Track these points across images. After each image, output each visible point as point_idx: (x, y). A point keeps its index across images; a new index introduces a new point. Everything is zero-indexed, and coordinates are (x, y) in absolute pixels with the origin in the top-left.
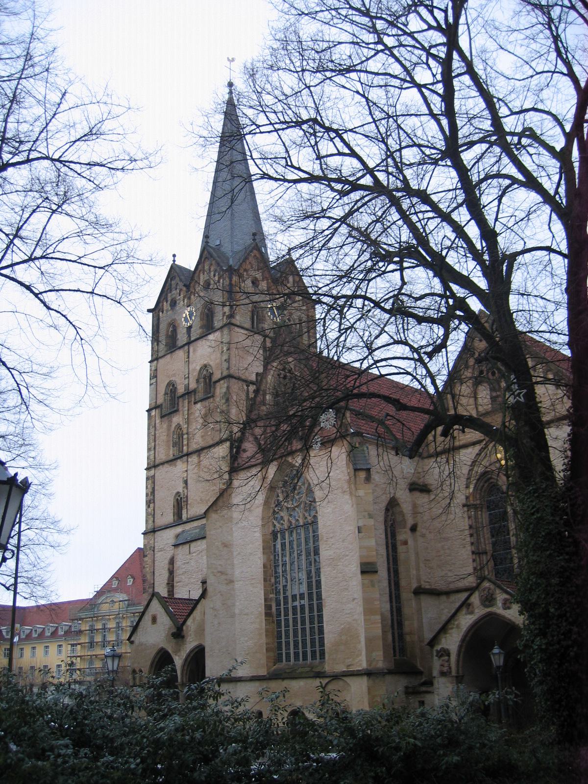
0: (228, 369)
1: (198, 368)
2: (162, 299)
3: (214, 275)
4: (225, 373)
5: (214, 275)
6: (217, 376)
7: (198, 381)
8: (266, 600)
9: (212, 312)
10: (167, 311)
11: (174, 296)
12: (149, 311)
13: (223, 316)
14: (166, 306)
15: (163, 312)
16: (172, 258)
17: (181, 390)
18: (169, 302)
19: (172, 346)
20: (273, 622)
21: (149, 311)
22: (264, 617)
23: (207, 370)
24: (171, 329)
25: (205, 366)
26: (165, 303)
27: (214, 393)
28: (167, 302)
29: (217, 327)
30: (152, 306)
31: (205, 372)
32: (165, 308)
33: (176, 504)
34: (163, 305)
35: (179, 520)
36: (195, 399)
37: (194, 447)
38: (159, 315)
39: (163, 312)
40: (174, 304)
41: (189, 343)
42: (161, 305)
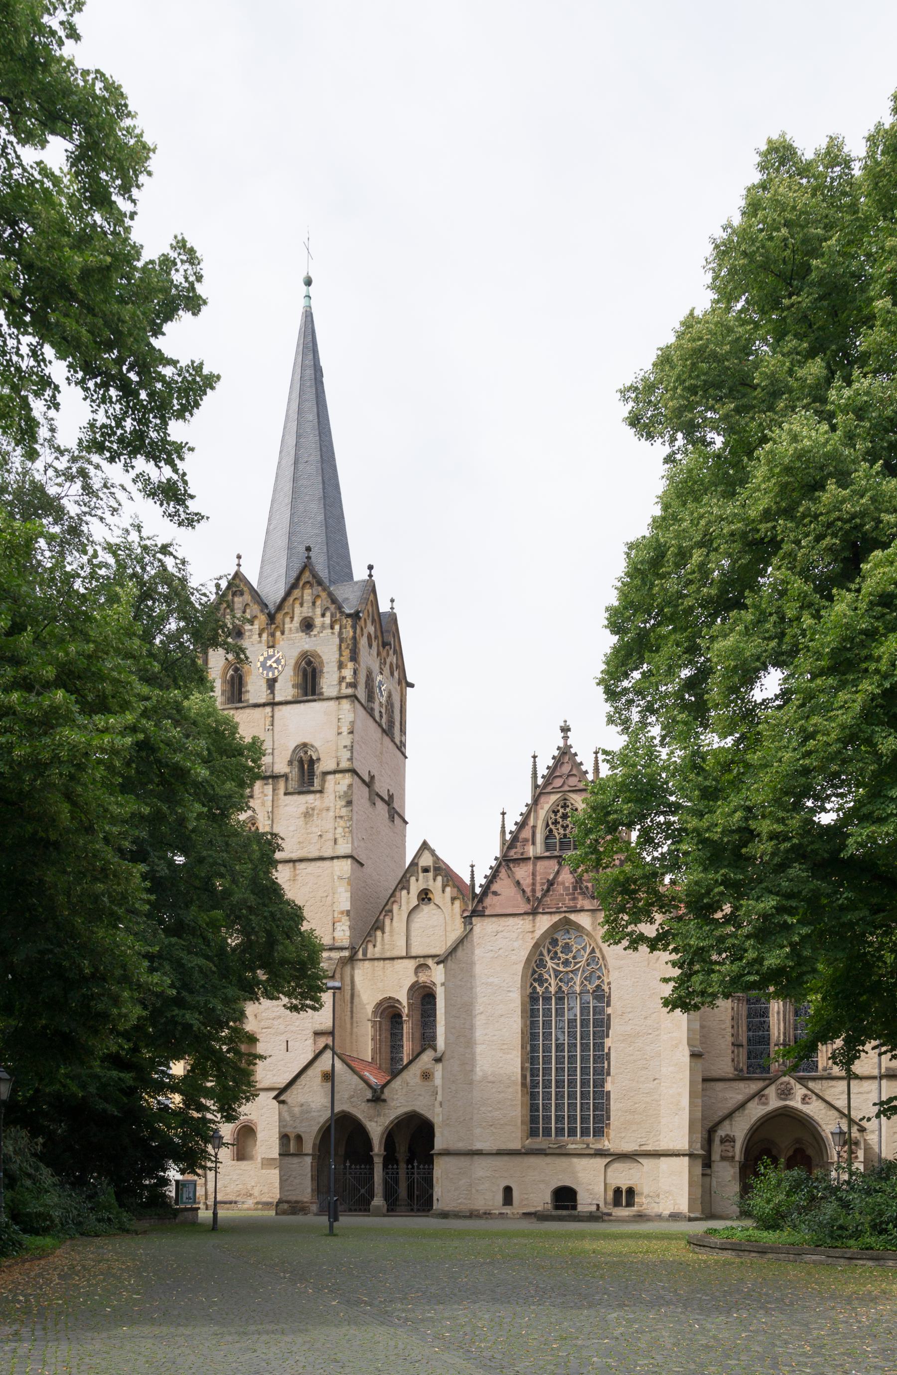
0: (351, 759)
3: (323, 615)
4: (345, 765)
5: (323, 615)
7: (290, 763)
9: (314, 670)
16: (236, 561)
23: (306, 753)
24: (231, 672)
25: (305, 745)
36: (286, 788)
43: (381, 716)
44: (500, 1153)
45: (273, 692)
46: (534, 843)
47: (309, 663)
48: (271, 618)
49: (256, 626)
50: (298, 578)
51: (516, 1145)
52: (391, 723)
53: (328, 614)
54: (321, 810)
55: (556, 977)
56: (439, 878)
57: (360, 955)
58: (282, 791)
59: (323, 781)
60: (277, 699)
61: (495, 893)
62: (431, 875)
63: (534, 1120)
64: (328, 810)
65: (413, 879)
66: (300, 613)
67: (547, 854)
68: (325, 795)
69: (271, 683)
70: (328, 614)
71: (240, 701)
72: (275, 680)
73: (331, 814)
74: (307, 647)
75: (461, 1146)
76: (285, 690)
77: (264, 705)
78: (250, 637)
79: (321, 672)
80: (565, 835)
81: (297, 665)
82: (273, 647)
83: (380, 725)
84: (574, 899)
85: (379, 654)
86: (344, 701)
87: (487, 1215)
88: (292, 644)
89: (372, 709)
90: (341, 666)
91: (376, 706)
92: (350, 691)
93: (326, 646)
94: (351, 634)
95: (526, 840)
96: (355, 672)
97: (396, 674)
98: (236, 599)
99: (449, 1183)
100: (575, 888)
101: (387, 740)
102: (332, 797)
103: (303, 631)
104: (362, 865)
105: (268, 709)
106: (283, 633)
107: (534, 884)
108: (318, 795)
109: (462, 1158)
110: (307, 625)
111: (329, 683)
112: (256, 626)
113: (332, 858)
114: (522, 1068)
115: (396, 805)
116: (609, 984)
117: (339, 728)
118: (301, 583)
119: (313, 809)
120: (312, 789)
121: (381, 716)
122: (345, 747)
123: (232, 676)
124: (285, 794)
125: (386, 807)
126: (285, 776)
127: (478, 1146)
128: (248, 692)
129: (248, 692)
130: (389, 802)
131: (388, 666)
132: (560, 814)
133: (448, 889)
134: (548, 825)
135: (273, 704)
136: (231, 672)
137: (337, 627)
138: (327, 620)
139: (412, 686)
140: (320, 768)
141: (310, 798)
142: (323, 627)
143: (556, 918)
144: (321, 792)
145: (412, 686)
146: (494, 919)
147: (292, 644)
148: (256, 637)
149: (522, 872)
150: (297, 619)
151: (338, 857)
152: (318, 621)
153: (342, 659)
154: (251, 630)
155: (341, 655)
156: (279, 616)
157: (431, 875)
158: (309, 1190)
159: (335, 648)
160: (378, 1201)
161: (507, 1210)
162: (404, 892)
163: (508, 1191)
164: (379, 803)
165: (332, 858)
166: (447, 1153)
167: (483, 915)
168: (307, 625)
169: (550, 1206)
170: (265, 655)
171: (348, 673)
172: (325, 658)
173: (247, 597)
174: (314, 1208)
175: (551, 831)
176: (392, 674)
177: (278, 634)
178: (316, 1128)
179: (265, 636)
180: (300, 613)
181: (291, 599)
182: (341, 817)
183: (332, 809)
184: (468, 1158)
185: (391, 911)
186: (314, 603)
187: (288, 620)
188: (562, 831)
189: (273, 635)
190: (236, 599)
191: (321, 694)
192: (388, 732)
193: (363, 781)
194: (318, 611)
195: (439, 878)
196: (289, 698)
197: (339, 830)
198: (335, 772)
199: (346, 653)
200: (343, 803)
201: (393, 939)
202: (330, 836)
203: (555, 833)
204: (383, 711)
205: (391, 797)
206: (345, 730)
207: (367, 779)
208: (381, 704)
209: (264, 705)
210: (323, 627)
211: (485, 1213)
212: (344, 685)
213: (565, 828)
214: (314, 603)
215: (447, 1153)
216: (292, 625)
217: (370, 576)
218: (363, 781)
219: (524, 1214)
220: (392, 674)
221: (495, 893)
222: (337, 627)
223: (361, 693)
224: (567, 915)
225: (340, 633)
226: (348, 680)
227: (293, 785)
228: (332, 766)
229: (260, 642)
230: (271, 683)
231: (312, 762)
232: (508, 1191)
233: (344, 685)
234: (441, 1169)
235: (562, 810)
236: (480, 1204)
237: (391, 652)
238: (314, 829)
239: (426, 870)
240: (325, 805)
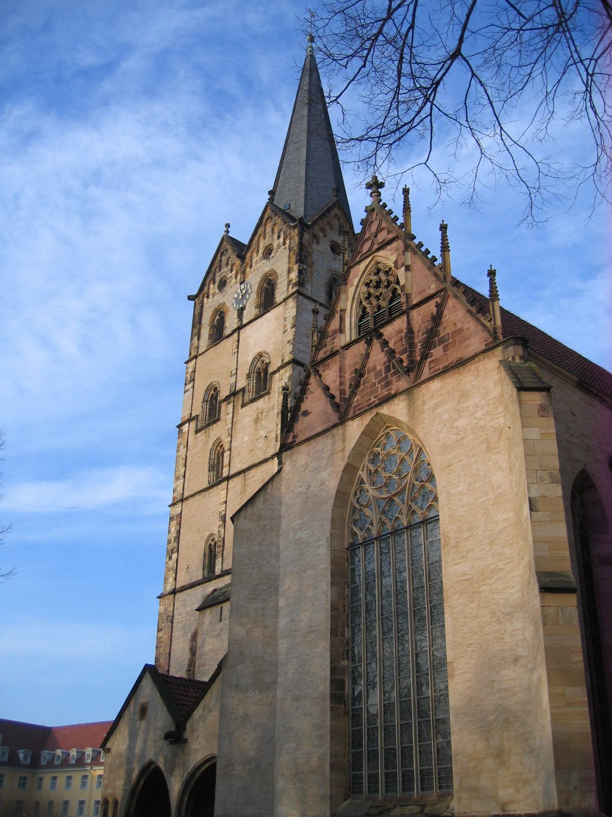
1: (250, 359)
2: (207, 282)
6: (275, 364)
7: (248, 376)
8: (333, 670)
10: (214, 295)
14: (213, 288)
17: (224, 393)
18: (217, 284)
19: (218, 334)
20: (346, 713)
22: (328, 703)
24: (217, 317)
29: (278, 302)
30: (195, 292)
31: (259, 365)
32: (211, 292)
33: (207, 551)
34: (209, 289)
35: (210, 575)
37: (237, 467)
38: (202, 302)
39: (208, 297)
40: (223, 284)
41: (239, 329)
42: (206, 288)
68: (272, 394)
69: (241, 311)
78: (230, 282)
90: (289, 271)
92: (295, 289)
111: (282, 291)
117: (285, 326)
122: (289, 342)
140: (270, 370)
148: (234, 281)
152: (275, 246)
154: (231, 277)
159: (286, 260)
171: (294, 276)
172: (279, 272)
177: (248, 269)
206: (289, 326)
226: (294, 281)
228: (279, 364)
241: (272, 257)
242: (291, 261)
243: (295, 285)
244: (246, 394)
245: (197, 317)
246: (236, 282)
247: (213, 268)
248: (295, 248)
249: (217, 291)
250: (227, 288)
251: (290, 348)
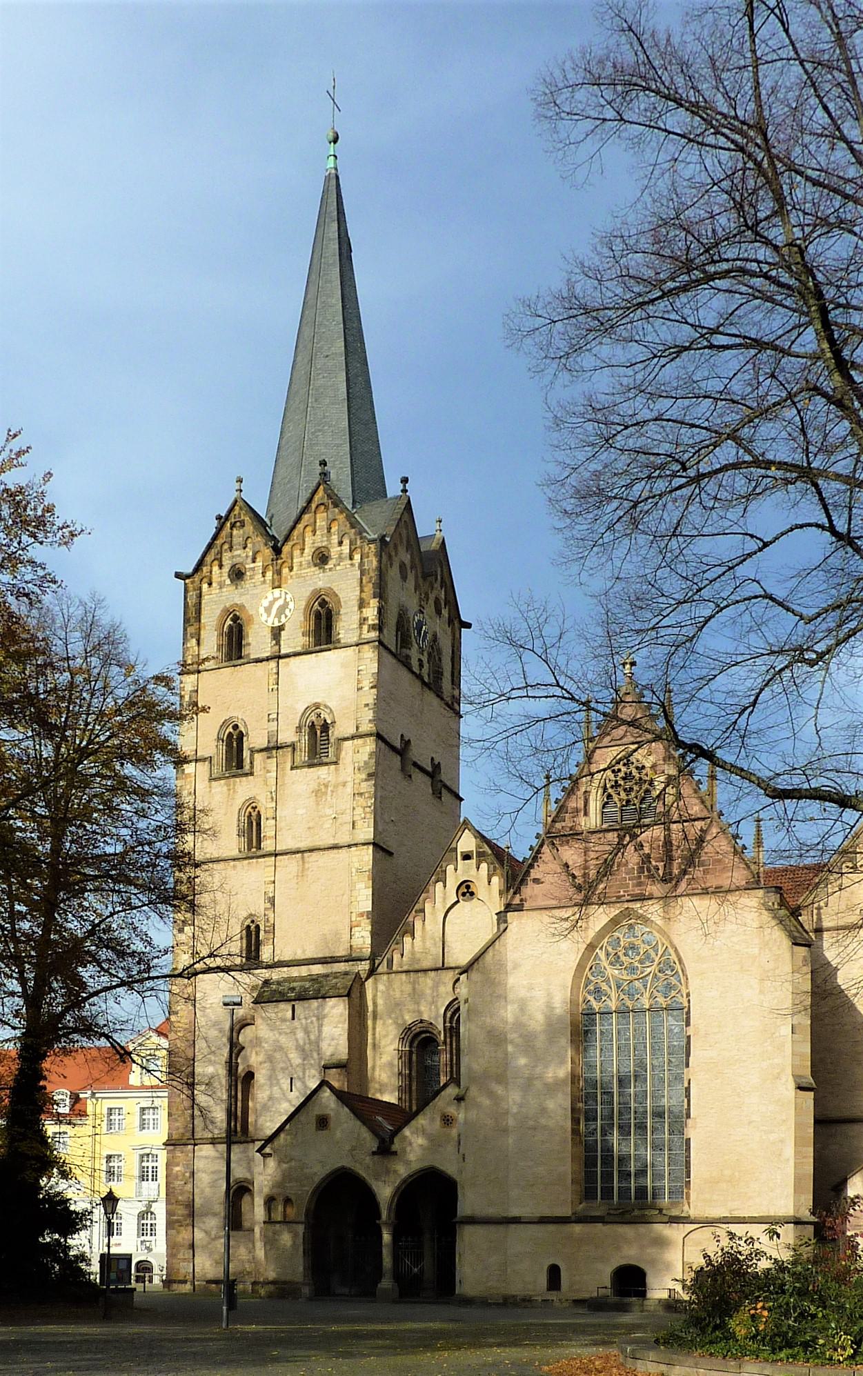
2: (209, 559)
3: (340, 543)
5: (340, 543)
6: (343, 728)
7: (299, 729)
11: (236, 561)
12: (178, 575)
13: (361, 624)
14: (219, 574)
15: (210, 584)
18: (226, 569)
21: (178, 575)
23: (319, 716)
24: (229, 622)
25: (317, 706)
26: (216, 569)
27: (338, 756)
28: (221, 566)
31: (313, 718)
32: (215, 578)
38: (200, 589)
42: (205, 569)
43: (421, 666)
44: (543, 1221)
45: (278, 643)
46: (586, 814)
47: (323, 603)
48: (277, 551)
49: (259, 564)
50: (310, 501)
51: (566, 1211)
52: (437, 674)
53: (346, 542)
54: (336, 786)
55: (618, 987)
56: (484, 866)
57: (383, 968)
58: (289, 765)
59: (338, 749)
60: (283, 652)
61: (536, 881)
62: (474, 861)
63: (590, 1177)
64: (344, 785)
65: (450, 868)
66: (312, 542)
67: (605, 826)
69: (277, 633)
70: (346, 542)
71: (240, 657)
72: (281, 628)
73: (349, 790)
74: (320, 584)
75: (491, 1211)
76: (294, 639)
77: (267, 659)
79: (338, 613)
80: (628, 801)
81: (308, 607)
82: (279, 587)
83: (419, 677)
84: (640, 884)
85: (417, 587)
86: (366, 647)
87: (527, 1302)
88: (303, 581)
89: (408, 657)
90: (362, 604)
91: (414, 653)
93: (346, 581)
94: (375, 563)
95: (577, 810)
96: (381, 611)
97: (445, 612)
98: (235, 532)
99: (479, 1262)
100: (641, 870)
101: (430, 697)
102: (350, 769)
103: (315, 565)
104: (390, 854)
105: (273, 664)
106: (291, 569)
107: (586, 868)
108: (333, 767)
109: (492, 1228)
110: (322, 558)
111: (347, 626)
112: (259, 564)
113: (349, 846)
114: (573, 1110)
115: (444, 776)
116: (688, 995)
118: (313, 506)
119: (326, 786)
120: (325, 760)
121: (421, 666)
122: (367, 705)
123: (230, 627)
124: (292, 769)
125: (428, 780)
126: (293, 746)
127: (515, 1212)
128: (249, 644)
129: (249, 644)
130: (434, 773)
131: (431, 602)
132: (621, 774)
133: (495, 880)
134: (605, 789)
135: (280, 657)
136: (229, 622)
137: (357, 557)
138: (346, 548)
139: (468, 626)
140: (335, 733)
141: (323, 771)
142: (340, 558)
143: (614, 911)
144: (336, 763)
145: (468, 626)
146: (535, 913)
147: (303, 581)
149: (571, 854)
150: (308, 551)
151: (356, 845)
152: (334, 551)
153: (364, 595)
154: (253, 569)
155: (362, 591)
156: (286, 549)
157: (474, 861)
158: (301, 1269)
160: (386, 1283)
161: (553, 1296)
162: (440, 885)
163: (554, 1272)
164: (418, 777)
165: (349, 846)
166: (472, 1221)
167: (519, 908)
168: (322, 558)
169: (609, 1292)
170: (270, 598)
171: (371, 613)
173: (249, 528)
174: (306, 1290)
175: (609, 796)
176: (439, 612)
177: (285, 571)
178: (309, 1189)
179: (269, 574)
180: (312, 542)
181: (300, 526)
182: (361, 794)
183: (350, 785)
184: (501, 1228)
185: (423, 911)
186: (329, 529)
187: (297, 553)
188: (623, 795)
189: (279, 573)
190: (235, 532)
191: (339, 641)
192: (433, 684)
193: (393, 748)
194: (335, 539)
195: (484, 866)
196: (299, 649)
197: (359, 811)
198: (353, 738)
199: (369, 589)
200: (364, 776)
201: (419, 943)
202: (349, 819)
203: (616, 798)
204: (425, 659)
205: (437, 767)
206: (366, 684)
207: (398, 744)
208: (421, 651)
209: (267, 659)
210: (340, 558)
211: (524, 1300)
212: (365, 627)
213: (628, 791)
214: (329, 529)
215: (472, 1221)
216: (302, 559)
217: (405, 491)
218: (393, 748)
219: (575, 1301)
220: (439, 612)
221: (536, 881)
222: (357, 557)
223: (391, 639)
224: (631, 905)
225: (361, 564)
226: (370, 622)
227: (302, 756)
229: (264, 582)
230: (277, 633)
231: (325, 727)
232: (554, 1272)
233: (365, 627)
234: (470, 1242)
235: (624, 769)
236: (516, 1288)
237: (437, 585)
238: (329, 811)
239: (467, 857)
240: (341, 780)
241: (330, 569)
242: (366, 589)
243: (372, 627)
244: (298, 753)
245: (192, 610)
246: (264, 582)
247: (218, 542)
248: (372, 574)
249: (228, 582)
250: (247, 584)
251: (370, 715)
